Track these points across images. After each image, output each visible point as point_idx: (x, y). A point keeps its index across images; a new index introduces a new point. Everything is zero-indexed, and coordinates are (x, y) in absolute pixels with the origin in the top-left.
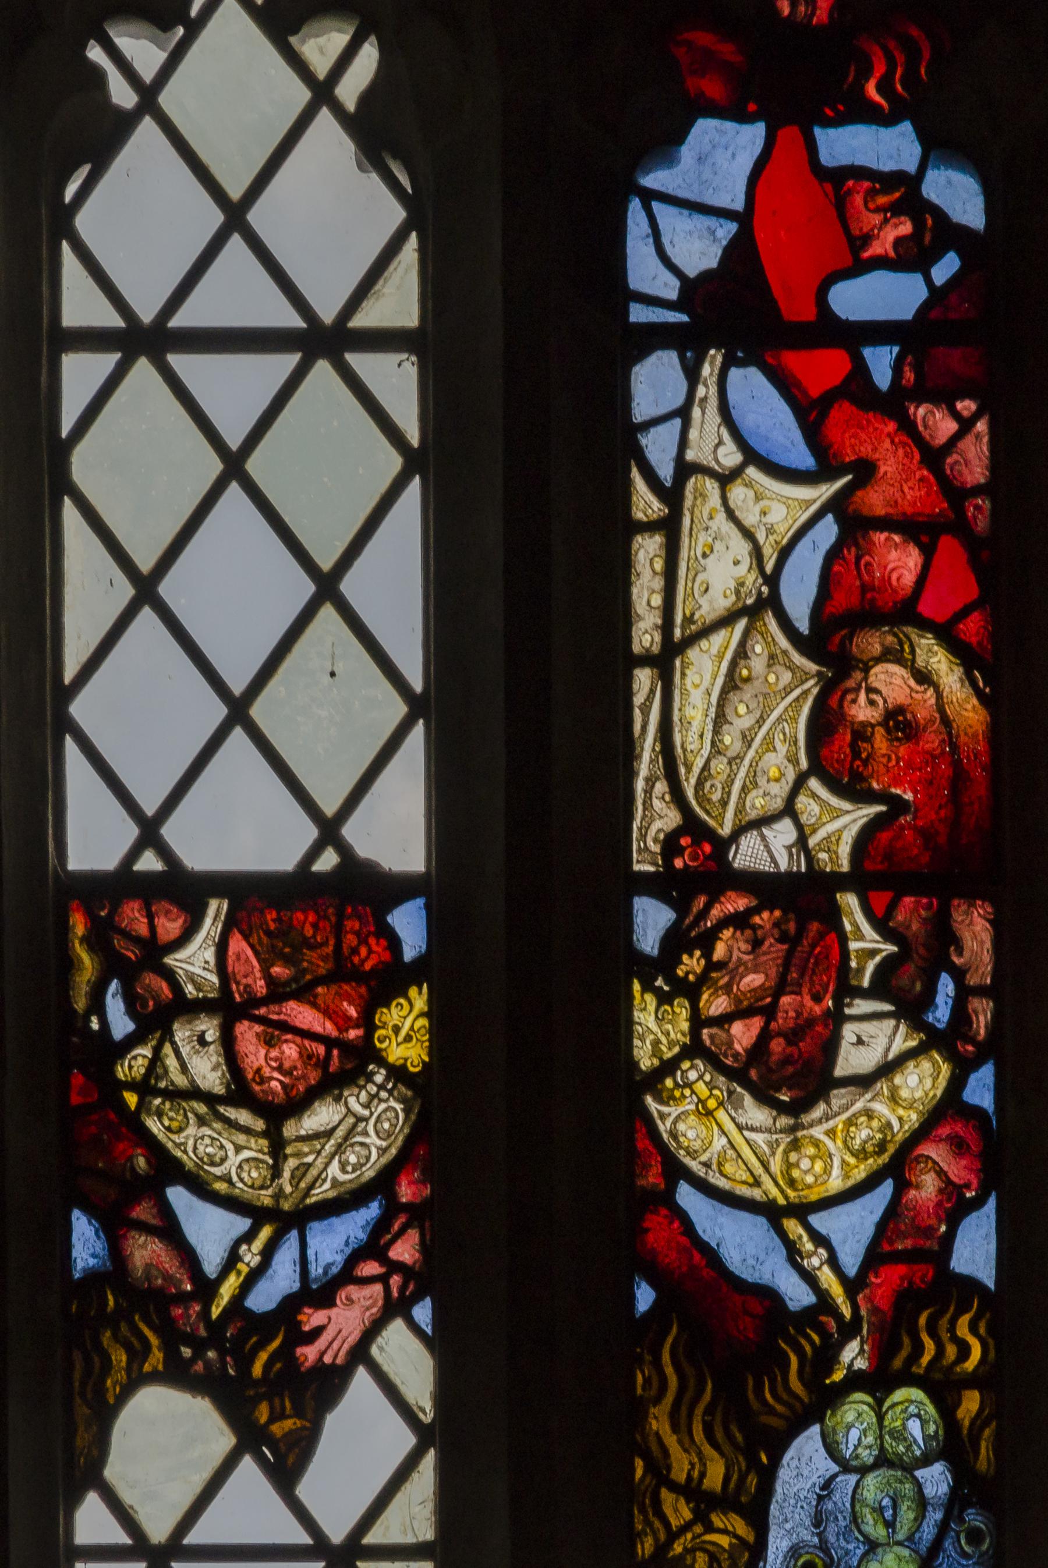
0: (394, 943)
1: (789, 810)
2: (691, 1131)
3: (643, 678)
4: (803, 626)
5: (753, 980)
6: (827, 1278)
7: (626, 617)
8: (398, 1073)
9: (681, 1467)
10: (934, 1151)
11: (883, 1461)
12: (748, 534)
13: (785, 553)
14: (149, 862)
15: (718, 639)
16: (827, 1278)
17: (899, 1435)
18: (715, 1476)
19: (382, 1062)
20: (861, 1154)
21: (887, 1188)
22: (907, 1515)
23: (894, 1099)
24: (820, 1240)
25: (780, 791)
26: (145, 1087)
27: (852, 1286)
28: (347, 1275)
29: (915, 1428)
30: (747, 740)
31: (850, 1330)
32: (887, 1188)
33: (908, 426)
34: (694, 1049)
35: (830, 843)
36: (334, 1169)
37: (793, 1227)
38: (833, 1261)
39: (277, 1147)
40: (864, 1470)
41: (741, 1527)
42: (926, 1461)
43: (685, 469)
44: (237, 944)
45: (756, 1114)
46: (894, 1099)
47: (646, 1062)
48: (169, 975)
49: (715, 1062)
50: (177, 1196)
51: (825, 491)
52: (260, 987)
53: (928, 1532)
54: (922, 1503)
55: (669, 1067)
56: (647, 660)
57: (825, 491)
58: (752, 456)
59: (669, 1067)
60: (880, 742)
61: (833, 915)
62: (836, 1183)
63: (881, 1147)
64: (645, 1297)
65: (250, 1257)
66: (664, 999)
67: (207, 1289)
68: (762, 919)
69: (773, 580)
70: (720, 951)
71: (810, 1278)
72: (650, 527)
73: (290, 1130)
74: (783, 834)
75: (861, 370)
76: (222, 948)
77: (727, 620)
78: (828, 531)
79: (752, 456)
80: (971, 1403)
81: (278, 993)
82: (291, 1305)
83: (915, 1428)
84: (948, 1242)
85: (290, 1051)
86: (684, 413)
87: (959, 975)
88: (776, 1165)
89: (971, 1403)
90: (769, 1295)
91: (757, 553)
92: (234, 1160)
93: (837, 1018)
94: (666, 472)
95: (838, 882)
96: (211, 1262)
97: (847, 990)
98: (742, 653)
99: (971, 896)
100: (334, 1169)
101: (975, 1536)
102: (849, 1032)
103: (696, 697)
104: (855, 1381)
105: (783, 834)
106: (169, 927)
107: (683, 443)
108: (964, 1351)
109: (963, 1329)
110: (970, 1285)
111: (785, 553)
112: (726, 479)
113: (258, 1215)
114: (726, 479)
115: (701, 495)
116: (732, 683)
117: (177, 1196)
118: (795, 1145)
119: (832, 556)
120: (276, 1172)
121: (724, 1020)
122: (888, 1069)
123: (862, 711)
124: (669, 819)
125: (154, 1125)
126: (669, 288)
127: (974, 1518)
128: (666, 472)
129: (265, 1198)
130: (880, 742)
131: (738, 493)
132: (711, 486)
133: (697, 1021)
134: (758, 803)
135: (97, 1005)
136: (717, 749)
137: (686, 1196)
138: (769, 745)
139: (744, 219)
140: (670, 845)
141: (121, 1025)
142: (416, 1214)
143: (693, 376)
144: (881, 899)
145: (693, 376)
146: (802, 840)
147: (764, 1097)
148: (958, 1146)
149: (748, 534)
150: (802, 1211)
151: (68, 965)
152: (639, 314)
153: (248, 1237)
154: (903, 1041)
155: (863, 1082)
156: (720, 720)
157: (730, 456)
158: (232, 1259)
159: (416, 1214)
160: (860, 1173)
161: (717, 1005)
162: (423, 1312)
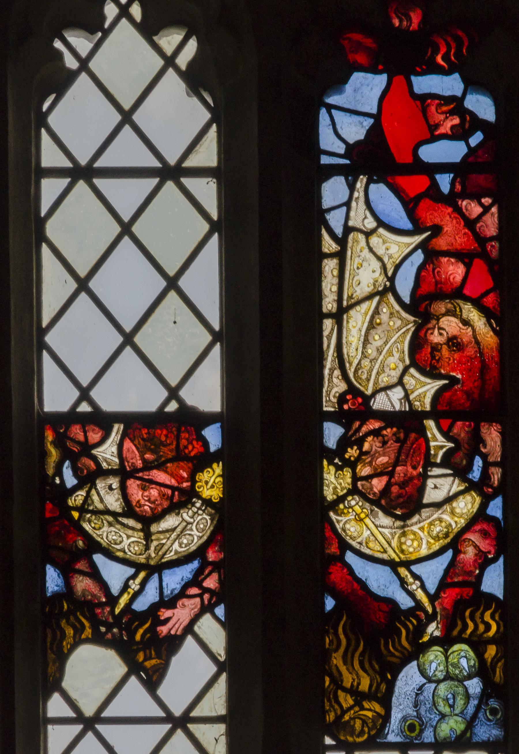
0: (206, 444)
1: (400, 382)
2: (352, 528)
3: (328, 324)
4: (407, 300)
5: (383, 460)
6: (420, 594)
7: (319, 296)
8: (207, 502)
9: (348, 680)
10: (473, 537)
11: (448, 677)
12: (379, 259)
13: (397, 267)
14: (84, 407)
15: (365, 306)
16: (420, 594)
17: (456, 666)
18: (365, 684)
19: (199, 497)
20: (437, 538)
21: (449, 554)
22: (460, 702)
23: (453, 513)
24: (416, 577)
25: (395, 375)
26: (82, 509)
27: (432, 598)
28: (182, 594)
29: (464, 662)
30: (379, 351)
31: (431, 618)
32: (449, 554)
33: (458, 210)
34: (354, 491)
35: (420, 398)
36: (176, 546)
37: (403, 571)
38: (423, 587)
39: (148, 536)
40: (439, 682)
41: (378, 708)
42: (470, 677)
43: (348, 230)
44: (128, 444)
45: (384, 520)
46: (453, 513)
47: (330, 496)
48: (94, 459)
49: (364, 496)
50: (98, 559)
51: (418, 239)
52: (139, 464)
53: (471, 710)
54: (468, 696)
55: (341, 499)
56: (330, 315)
57: (418, 239)
58: (381, 223)
59: (341, 499)
60: (445, 352)
61: (422, 431)
62: (424, 551)
63: (447, 535)
64: (330, 603)
65: (135, 585)
66: (339, 468)
67: (113, 600)
68: (388, 432)
69: (392, 279)
70: (366, 447)
71: (411, 595)
72: (331, 256)
73: (154, 528)
74: (397, 394)
75: (435, 185)
76: (120, 446)
77: (369, 297)
78: (419, 257)
79: (381, 223)
80: (491, 651)
81: (148, 466)
82: (155, 608)
83: (464, 662)
84: (480, 578)
85: (154, 492)
86: (348, 204)
87: (484, 457)
88: (395, 543)
89: (491, 651)
90: (392, 603)
91: (384, 267)
92: (126, 542)
93: (425, 477)
94: (339, 231)
95: (425, 415)
96: (115, 588)
97: (429, 463)
98: (377, 312)
99: (490, 421)
100: (176, 546)
101: (494, 712)
102: (430, 483)
103: (354, 332)
104: (434, 641)
105: (397, 394)
106: (94, 436)
107: (347, 218)
108: (488, 627)
109: (487, 617)
110: (491, 597)
111: (397, 267)
112: (368, 234)
113: (138, 567)
114: (368, 234)
115: (356, 241)
116: (372, 326)
117: (98, 559)
118: (404, 534)
119: (421, 268)
120: (147, 547)
121: (368, 478)
122: (449, 499)
123: (436, 338)
124: (341, 387)
125: (87, 526)
126: (341, 149)
127: (493, 703)
128: (339, 231)
129: (142, 559)
130: (445, 352)
131: (374, 240)
132: (361, 237)
133: (355, 478)
134: (385, 380)
135: (59, 472)
136: (364, 355)
137: (350, 557)
138: (390, 353)
139: (377, 117)
140: (342, 399)
141: (70, 481)
142: (216, 566)
143: (352, 187)
144: (446, 423)
145: (352, 187)
146: (407, 396)
147: (388, 512)
148: (485, 534)
149: (379, 259)
150: (407, 564)
151: (44, 454)
152: (325, 160)
153: (133, 577)
154: (457, 486)
155: (438, 505)
156: (366, 342)
157: (370, 223)
158: (126, 587)
159: (216, 566)
160: (436, 547)
161: (365, 471)
162: (220, 611)
